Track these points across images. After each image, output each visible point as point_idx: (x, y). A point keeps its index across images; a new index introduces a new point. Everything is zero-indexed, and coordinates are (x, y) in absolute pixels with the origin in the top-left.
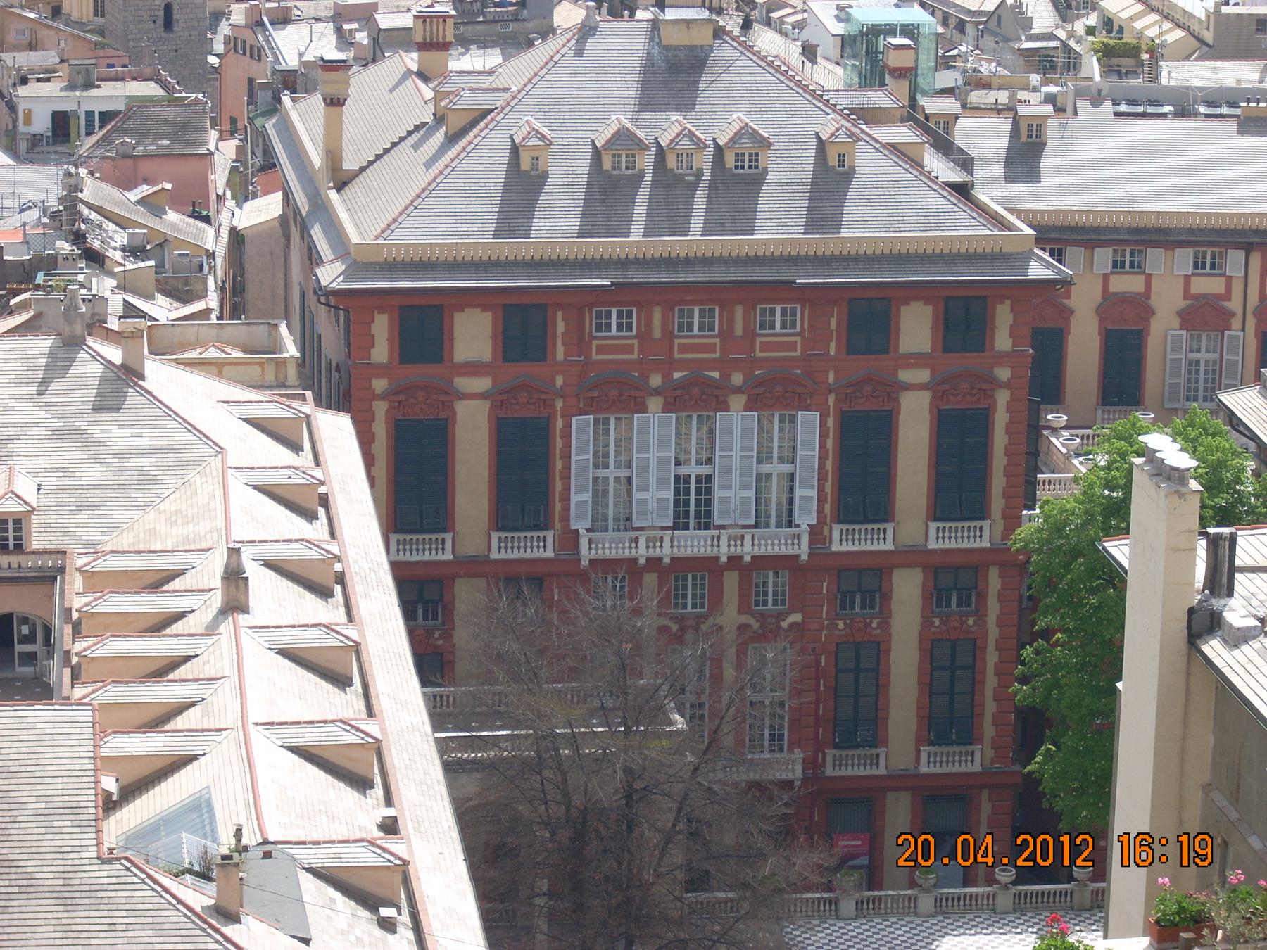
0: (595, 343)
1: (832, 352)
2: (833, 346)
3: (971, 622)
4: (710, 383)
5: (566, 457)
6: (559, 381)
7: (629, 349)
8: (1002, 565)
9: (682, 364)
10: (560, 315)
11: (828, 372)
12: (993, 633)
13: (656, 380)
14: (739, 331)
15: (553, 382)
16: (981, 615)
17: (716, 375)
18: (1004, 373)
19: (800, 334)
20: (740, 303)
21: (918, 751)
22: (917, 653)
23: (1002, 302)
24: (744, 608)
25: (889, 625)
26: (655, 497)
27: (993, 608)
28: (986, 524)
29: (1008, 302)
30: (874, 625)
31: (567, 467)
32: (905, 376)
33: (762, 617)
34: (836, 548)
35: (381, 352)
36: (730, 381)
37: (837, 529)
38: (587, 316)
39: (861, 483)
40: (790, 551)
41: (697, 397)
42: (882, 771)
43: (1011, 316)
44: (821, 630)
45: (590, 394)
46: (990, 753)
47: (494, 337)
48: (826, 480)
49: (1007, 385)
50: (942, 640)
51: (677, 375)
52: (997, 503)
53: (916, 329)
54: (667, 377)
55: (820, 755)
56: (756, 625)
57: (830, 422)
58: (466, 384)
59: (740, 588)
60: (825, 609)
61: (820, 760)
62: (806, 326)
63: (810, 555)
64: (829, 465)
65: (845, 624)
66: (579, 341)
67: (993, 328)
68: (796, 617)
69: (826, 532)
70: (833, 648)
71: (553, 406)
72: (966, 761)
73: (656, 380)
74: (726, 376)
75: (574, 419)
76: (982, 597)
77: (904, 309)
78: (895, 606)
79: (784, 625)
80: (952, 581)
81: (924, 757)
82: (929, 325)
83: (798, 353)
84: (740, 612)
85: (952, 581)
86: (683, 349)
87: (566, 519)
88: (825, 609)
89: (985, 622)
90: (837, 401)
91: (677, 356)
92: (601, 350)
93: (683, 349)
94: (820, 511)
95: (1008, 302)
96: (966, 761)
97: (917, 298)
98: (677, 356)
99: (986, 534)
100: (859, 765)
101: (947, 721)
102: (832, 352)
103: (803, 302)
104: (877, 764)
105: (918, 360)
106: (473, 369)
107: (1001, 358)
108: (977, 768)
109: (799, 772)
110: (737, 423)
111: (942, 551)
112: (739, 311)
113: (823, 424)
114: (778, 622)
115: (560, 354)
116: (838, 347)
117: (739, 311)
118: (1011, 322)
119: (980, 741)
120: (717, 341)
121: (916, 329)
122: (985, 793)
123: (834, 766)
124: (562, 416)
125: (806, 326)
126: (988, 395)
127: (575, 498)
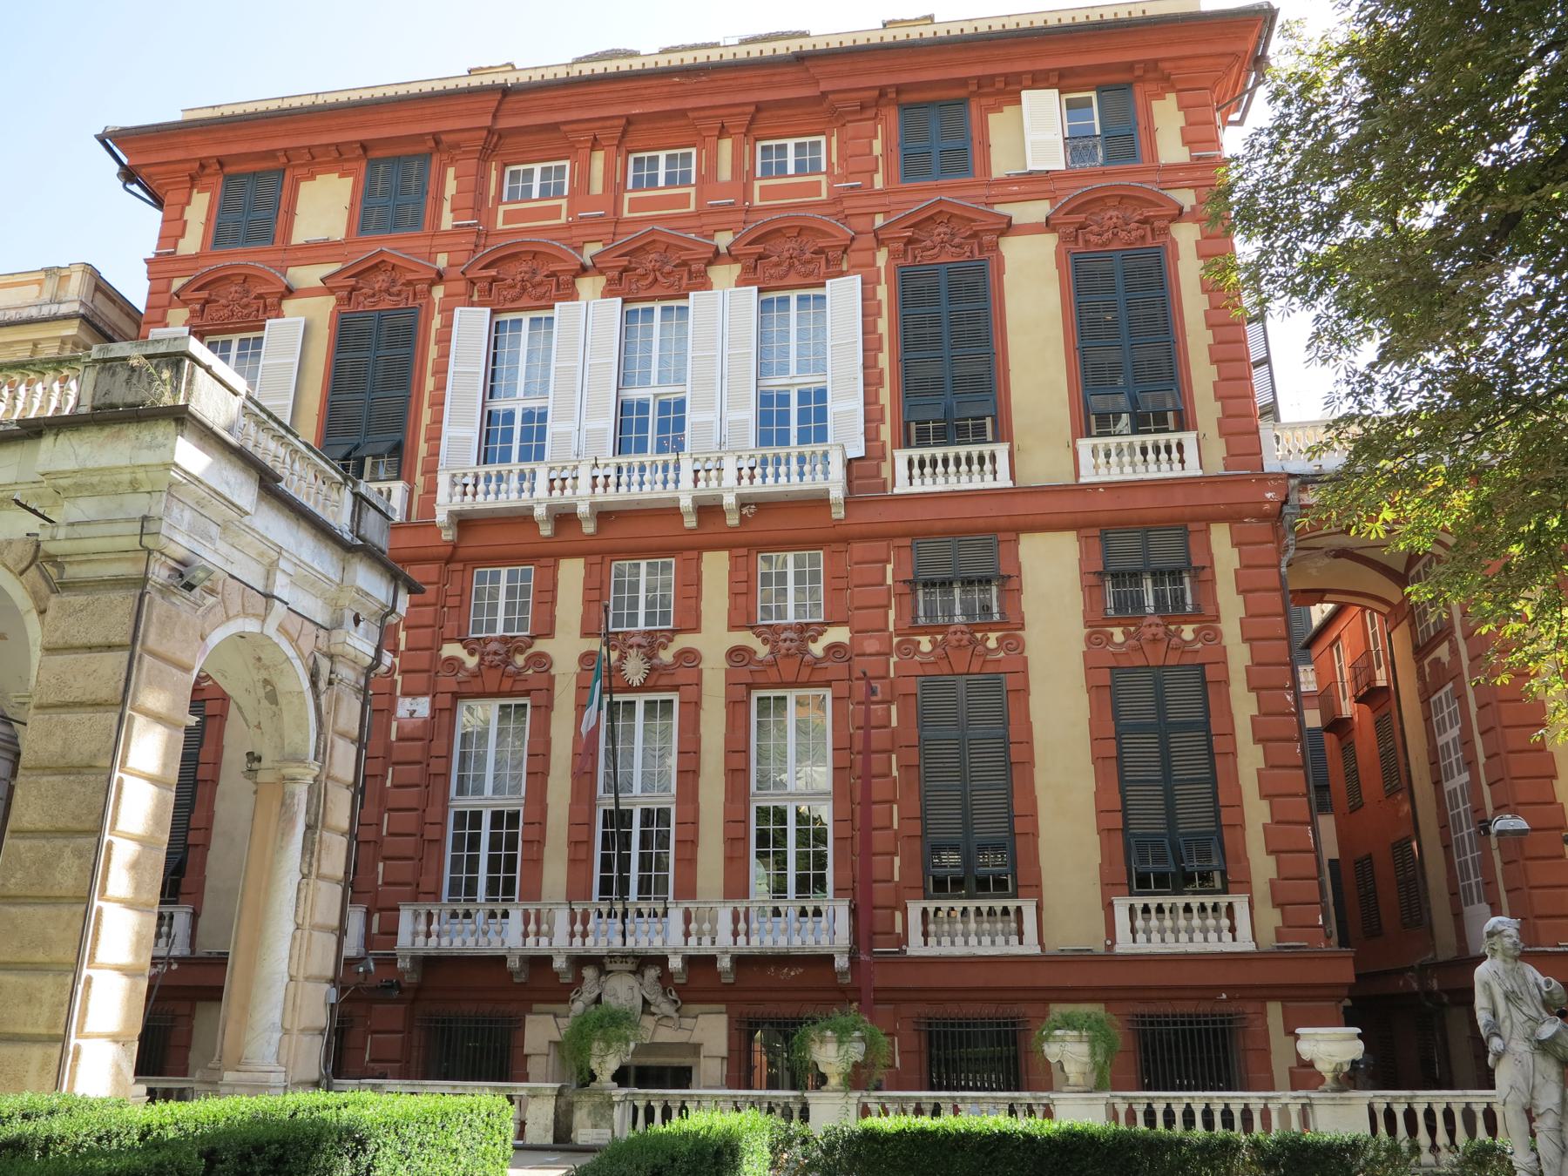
1: (879, 182)
3: (1188, 632)
5: (441, 371)
8: (1232, 517)
12: (1239, 656)
14: (725, 174)
16: (1207, 618)
19: (829, 173)
21: (1109, 908)
22: (1084, 700)
23: (1161, 97)
24: (741, 619)
25: (1020, 645)
26: (581, 428)
27: (1231, 606)
28: (1189, 438)
30: (992, 644)
31: (441, 387)
33: (771, 634)
34: (902, 487)
35: (191, 244)
37: (901, 456)
38: (494, 173)
39: (944, 378)
40: (809, 484)
41: (653, 271)
42: (1031, 947)
44: (888, 654)
46: (1271, 918)
48: (881, 384)
49: (1194, 217)
50: (1134, 669)
52: (1207, 409)
55: (898, 916)
56: (763, 651)
57: (882, 292)
58: (308, 275)
59: (731, 582)
61: (899, 929)
62: (834, 159)
63: (847, 502)
64: (884, 360)
65: (934, 643)
66: (477, 201)
67: (1151, 131)
68: (840, 635)
69: (886, 472)
70: (913, 686)
73: (592, 249)
75: (457, 310)
76: (1204, 576)
78: (1031, 604)
79: (817, 649)
80: (1139, 552)
84: (733, 627)
85: (1139, 552)
87: (431, 470)
89: (1218, 634)
90: (893, 255)
91: (626, 214)
94: (871, 436)
96: (1218, 930)
98: (626, 214)
99: (1191, 454)
101: (1166, 851)
104: (1020, 933)
106: (315, 251)
108: (1245, 944)
109: (843, 938)
110: (724, 308)
111: (1111, 487)
113: (868, 296)
114: (803, 641)
115: (447, 222)
116: (887, 180)
117: (726, 146)
119: (1245, 885)
123: (925, 934)
125: (834, 159)
127: (448, 431)
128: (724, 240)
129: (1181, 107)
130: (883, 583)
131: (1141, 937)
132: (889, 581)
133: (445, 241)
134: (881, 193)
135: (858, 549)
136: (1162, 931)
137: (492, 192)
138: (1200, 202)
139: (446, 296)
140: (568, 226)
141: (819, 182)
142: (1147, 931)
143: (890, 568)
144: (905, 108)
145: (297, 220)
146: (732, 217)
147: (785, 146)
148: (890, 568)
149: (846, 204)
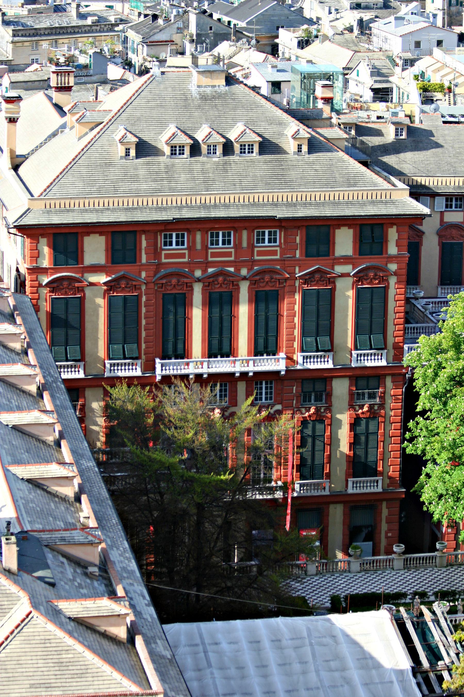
0: (164, 252)
2: (298, 252)
4: (229, 274)
6: (144, 274)
7: (183, 256)
8: (393, 375)
9: (213, 264)
10: (143, 237)
11: (295, 267)
13: (198, 273)
15: (140, 275)
17: (232, 269)
18: (393, 267)
19: (280, 246)
20: (246, 229)
21: (347, 481)
23: (392, 227)
29: (395, 227)
32: (339, 269)
36: (240, 273)
38: (159, 237)
43: (397, 234)
45: (161, 282)
47: (107, 250)
49: (395, 274)
51: (210, 270)
53: (344, 243)
54: (204, 271)
60: (295, 402)
62: (282, 241)
66: (155, 252)
71: (140, 289)
72: (374, 486)
73: (198, 273)
74: (238, 270)
77: (337, 231)
81: (350, 484)
82: (352, 240)
83: (278, 257)
86: (214, 255)
88: (295, 402)
92: (167, 256)
93: (214, 255)
95: (395, 227)
96: (374, 486)
97: (344, 225)
98: (210, 259)
100: (314, 489)
102: (298, 256)
103: (281, 228)
105: (345, 260)
107: (391, 259)
108: (380, 489)
112: (245, 234)
115: (144, 260)
116: (301, 254)
117: (245, 234)
118: (397, 238)
120: (233, 250)
121: (344, 243)
122: (384, 504)
124: (145, 295)
125: (282, 241)
126: (385, 280)
128: (244, 272)
129: (397, 232)
130: (292, 393)
131: (355, 488)
132: (294, 392)
133: (144, 267)
134: (299, 260)
135: (286, 382)
136: (360, 487)
137: (159, 246)
138: (399, 269)
139: (146, 288)
140: (188, 263)
141: (277, 250)
142: (356, 487)
143: (295, 388)
144: (307, 227)
145: (85, 254)
146: (247, 263)
147: (265, 232)
148: (295, 388)
149: (286, 262)
